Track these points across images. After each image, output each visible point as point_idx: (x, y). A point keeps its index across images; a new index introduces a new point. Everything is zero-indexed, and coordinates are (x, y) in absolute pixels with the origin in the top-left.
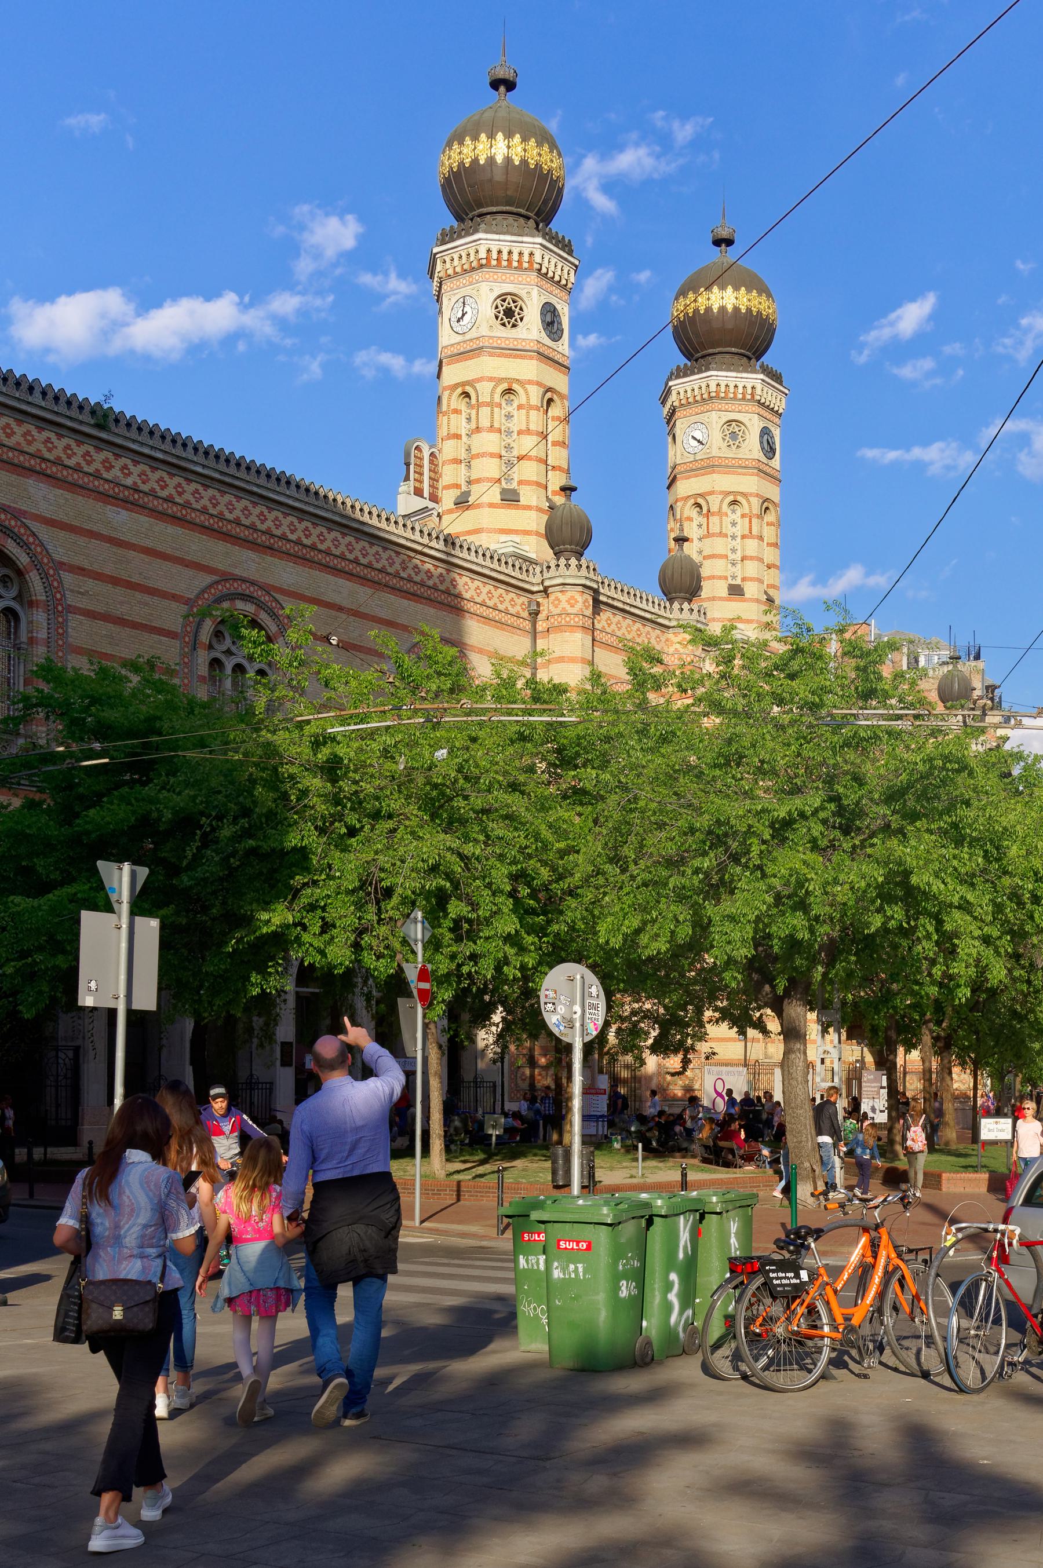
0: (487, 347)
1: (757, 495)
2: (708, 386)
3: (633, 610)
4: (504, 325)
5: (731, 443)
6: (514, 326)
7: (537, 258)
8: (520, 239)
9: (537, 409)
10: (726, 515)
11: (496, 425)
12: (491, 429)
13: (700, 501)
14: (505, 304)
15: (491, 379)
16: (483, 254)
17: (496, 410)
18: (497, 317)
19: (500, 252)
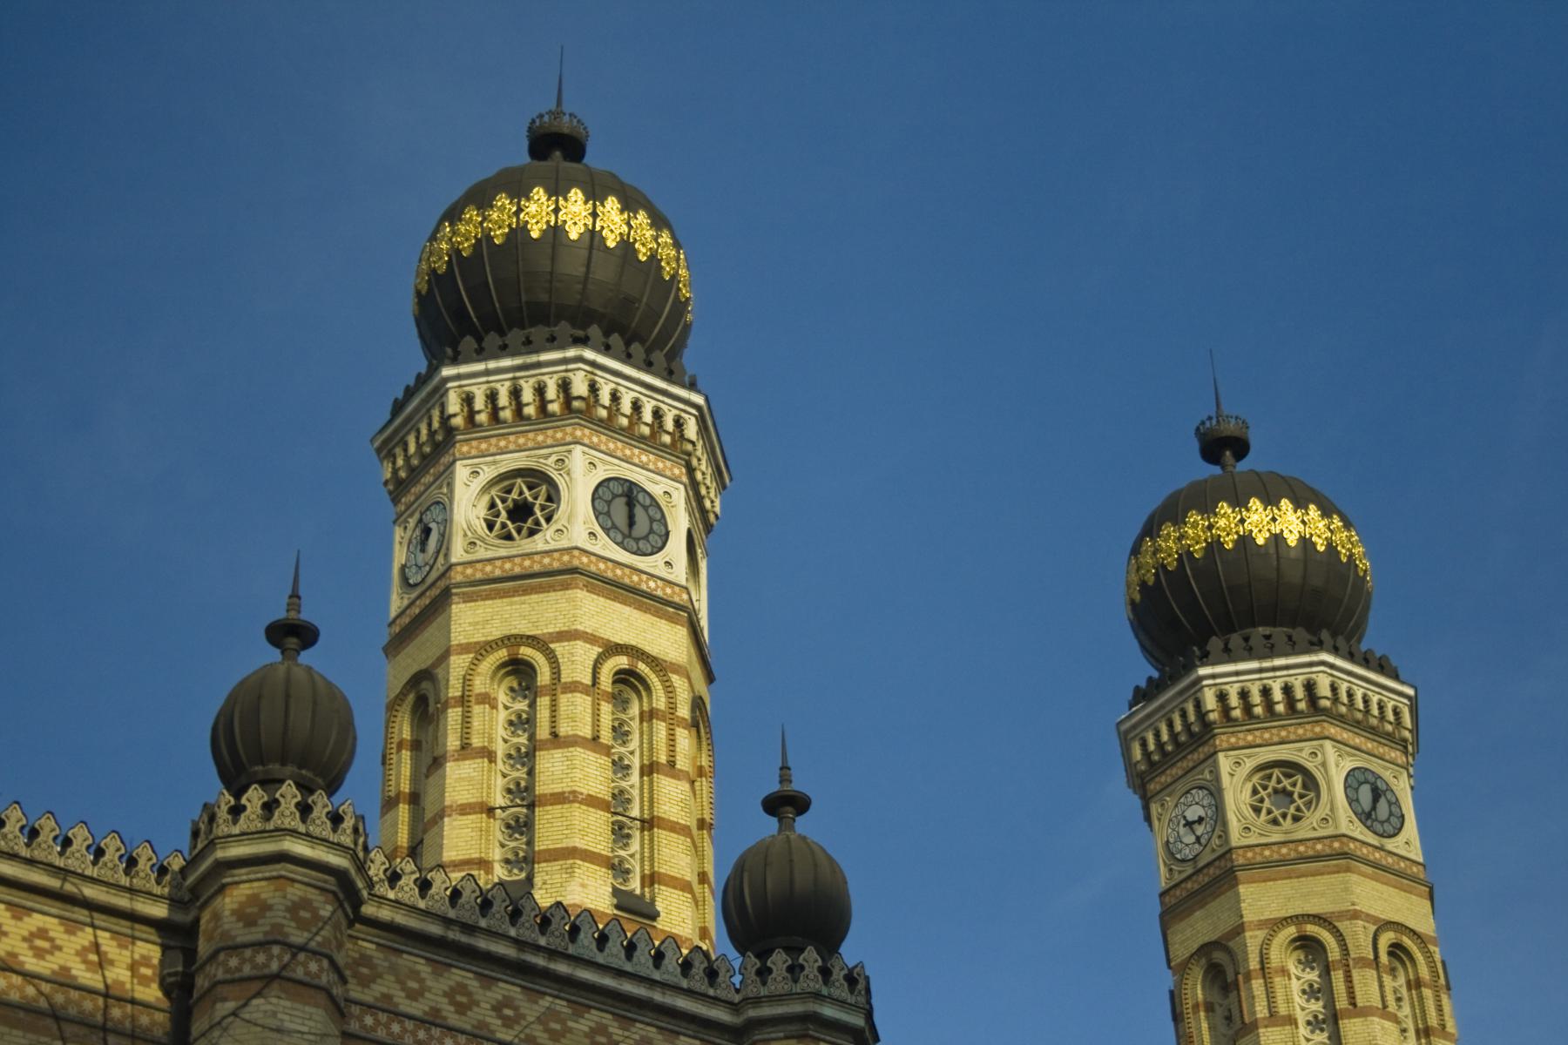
0: (458, 585)
1: (1355, 915)
2: (1198, 705)
3: (562, 968)
4: (509, 537)
5: (1277, 813)
6: (532, 533)
7: (580, 387)
8: (533, 359)
9: (586, 690)
10: (1284, 972)
11: (476, 742)
12: (465, 749)
13: (1219, 956)
14: (514, 495)
15: (465, 648)
16: (454, 405)
17: (477, 709)
18: (491, 526)
19: (492, 397)
